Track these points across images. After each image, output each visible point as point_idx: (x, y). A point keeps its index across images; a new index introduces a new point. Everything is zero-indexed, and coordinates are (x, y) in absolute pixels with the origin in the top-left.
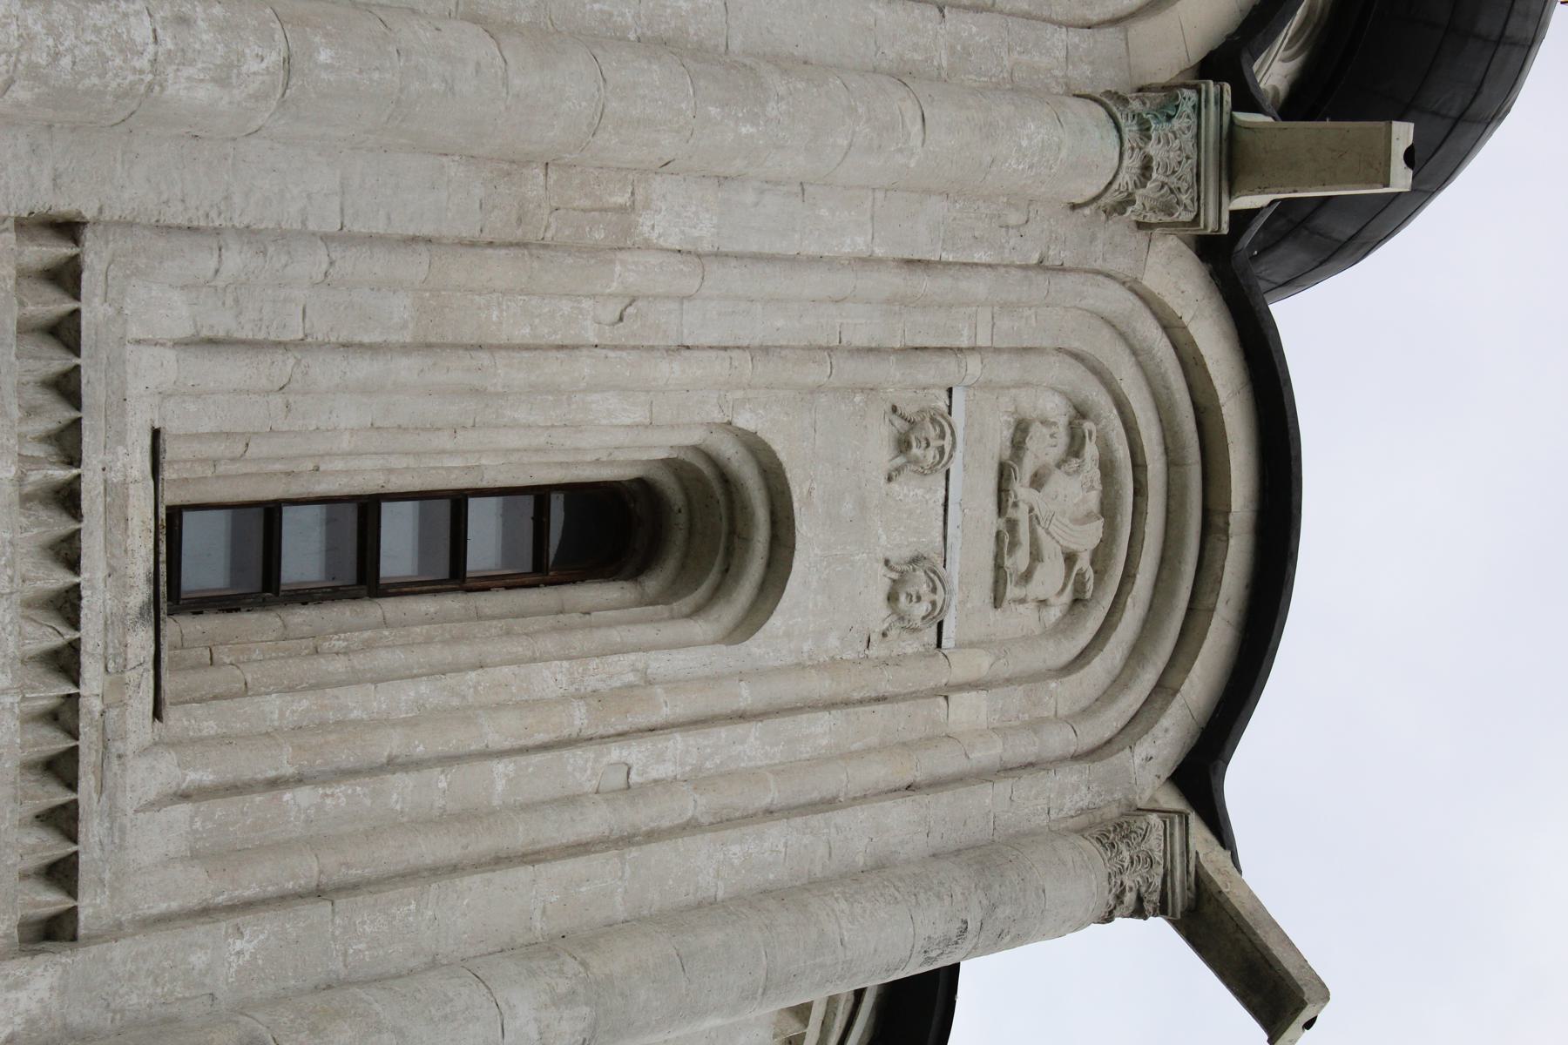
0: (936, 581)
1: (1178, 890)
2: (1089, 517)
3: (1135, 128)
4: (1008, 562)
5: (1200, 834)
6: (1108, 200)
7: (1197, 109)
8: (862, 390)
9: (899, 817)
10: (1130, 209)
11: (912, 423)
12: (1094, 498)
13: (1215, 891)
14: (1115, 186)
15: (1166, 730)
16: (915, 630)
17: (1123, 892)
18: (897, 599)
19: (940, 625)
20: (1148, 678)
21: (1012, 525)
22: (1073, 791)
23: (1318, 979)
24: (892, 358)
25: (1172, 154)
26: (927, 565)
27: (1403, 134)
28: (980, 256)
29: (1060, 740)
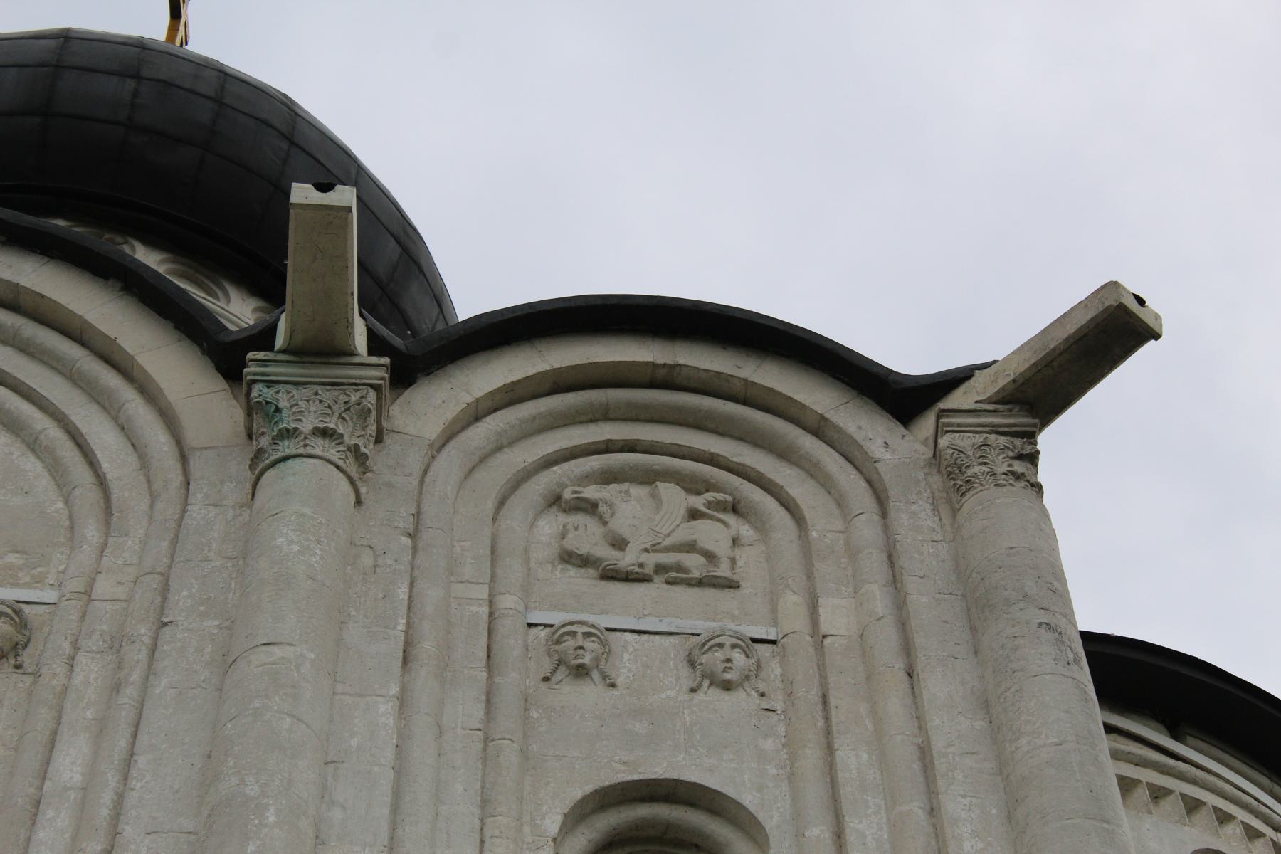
0: (711, 643)
1: (1011, 421)
2: (655, 496)
3: (286, 443)
4: (696, 574)
5: (959, 399)
6: (352, 469)
7: (270, 384)
8: (526, 710)
9: (936, 685)
10: (363, 450)
11: (560, 663)
12: (637, 491)
13: (1013, 386)
14: (340, 463)
15: (860, 428)
16: (759, 666)
17: (1013, 473)
18: (729, 682)
19: (755, 641)
20: (808, 443)
21: (661, 569)
22: (916, 517)
23: (1097, 291)
24: (497, 680)
25: (312, 409)
26: (696, 652)
27: (302, 193)
28: (402, 593)
29: (867, 529)
